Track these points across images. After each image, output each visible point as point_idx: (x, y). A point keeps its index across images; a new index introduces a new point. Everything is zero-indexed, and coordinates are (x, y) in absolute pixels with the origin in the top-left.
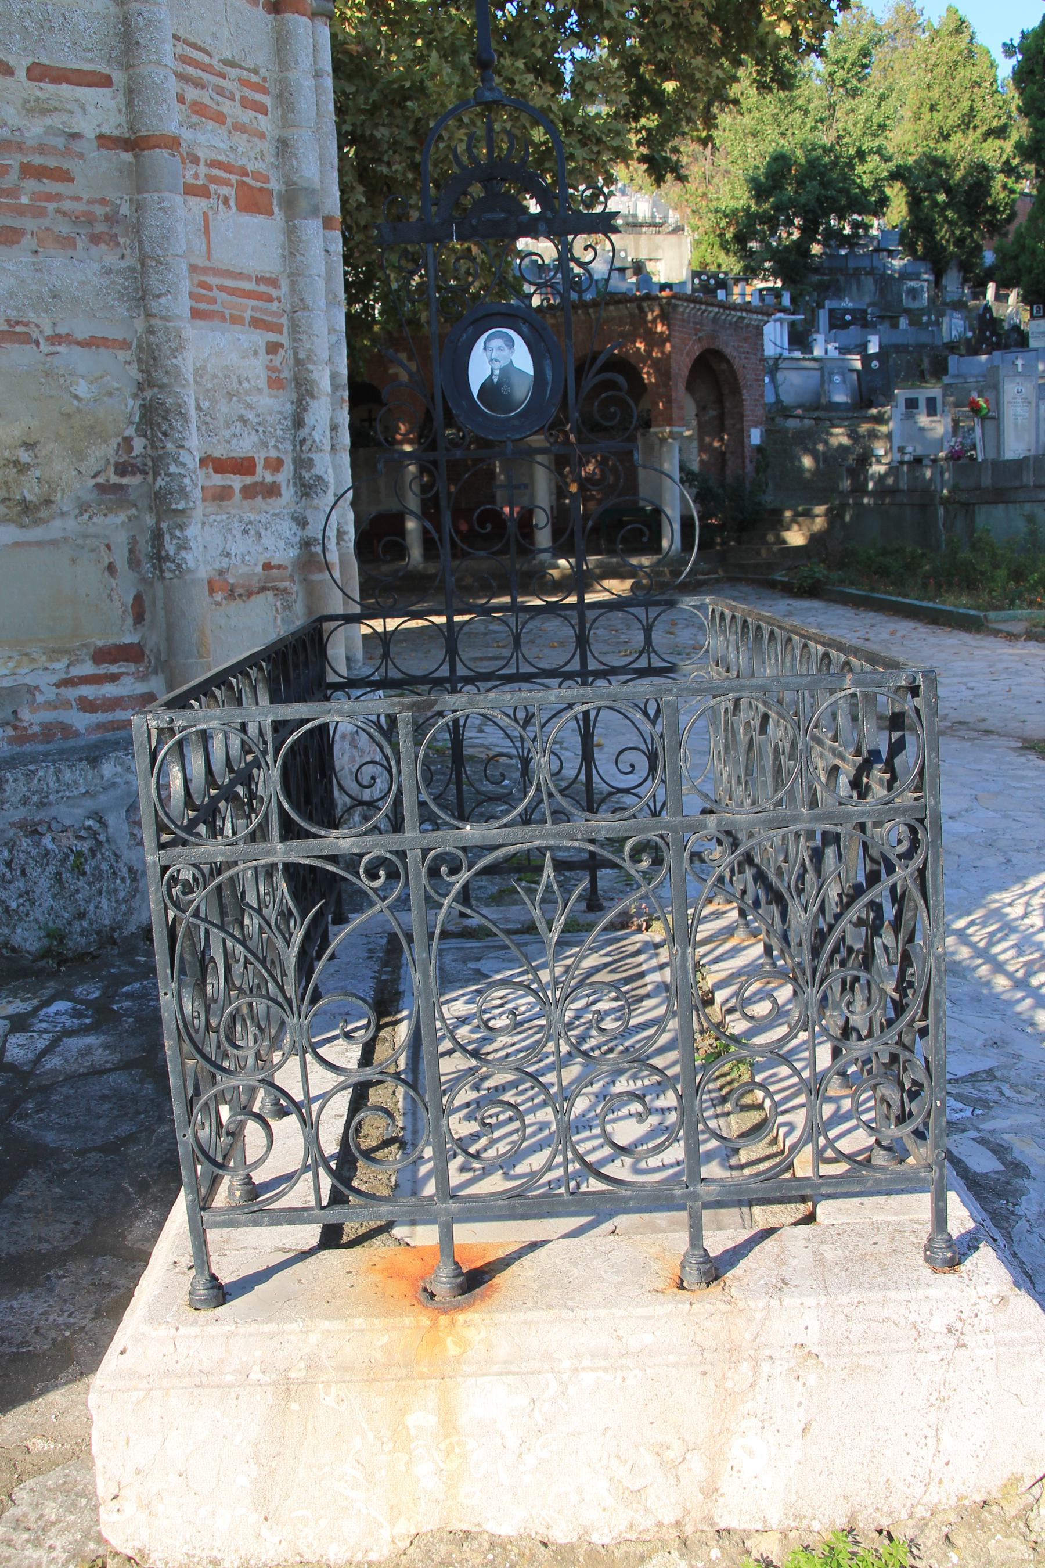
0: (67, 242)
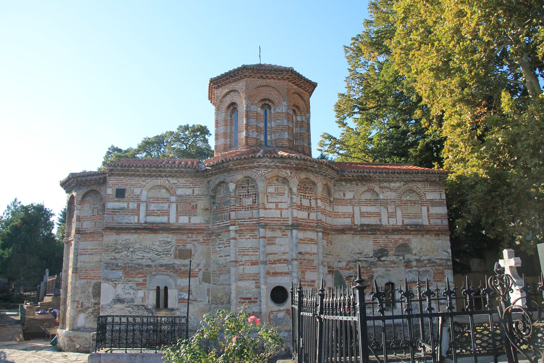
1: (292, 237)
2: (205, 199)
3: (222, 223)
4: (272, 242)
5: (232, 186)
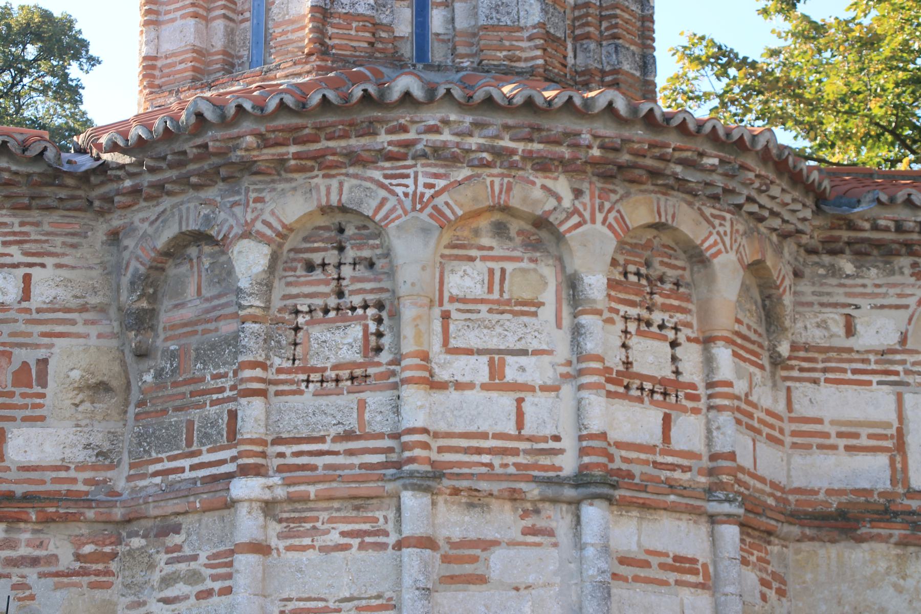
1: (580, 546)
2: (93, 331)
3: (186, 463)
4: (468, 568)
5: (250, 260)
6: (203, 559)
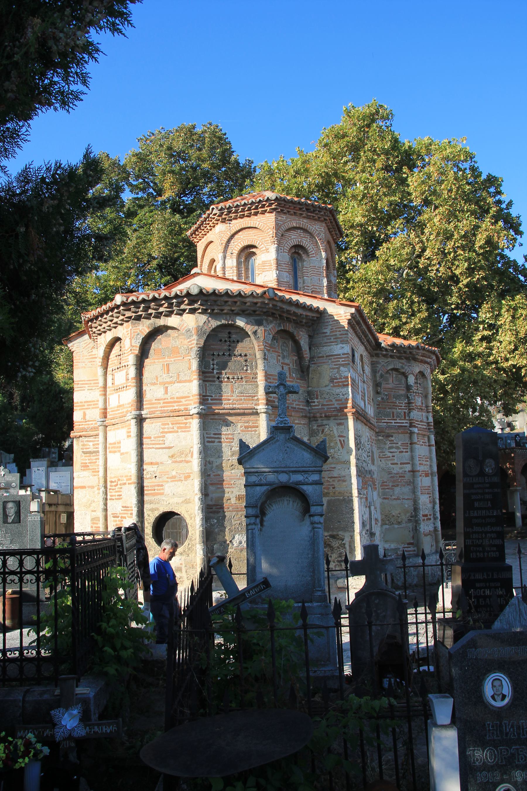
0: (404, 486)
3: (393, 421)
6: (400, 444)
